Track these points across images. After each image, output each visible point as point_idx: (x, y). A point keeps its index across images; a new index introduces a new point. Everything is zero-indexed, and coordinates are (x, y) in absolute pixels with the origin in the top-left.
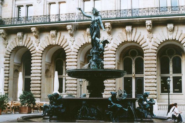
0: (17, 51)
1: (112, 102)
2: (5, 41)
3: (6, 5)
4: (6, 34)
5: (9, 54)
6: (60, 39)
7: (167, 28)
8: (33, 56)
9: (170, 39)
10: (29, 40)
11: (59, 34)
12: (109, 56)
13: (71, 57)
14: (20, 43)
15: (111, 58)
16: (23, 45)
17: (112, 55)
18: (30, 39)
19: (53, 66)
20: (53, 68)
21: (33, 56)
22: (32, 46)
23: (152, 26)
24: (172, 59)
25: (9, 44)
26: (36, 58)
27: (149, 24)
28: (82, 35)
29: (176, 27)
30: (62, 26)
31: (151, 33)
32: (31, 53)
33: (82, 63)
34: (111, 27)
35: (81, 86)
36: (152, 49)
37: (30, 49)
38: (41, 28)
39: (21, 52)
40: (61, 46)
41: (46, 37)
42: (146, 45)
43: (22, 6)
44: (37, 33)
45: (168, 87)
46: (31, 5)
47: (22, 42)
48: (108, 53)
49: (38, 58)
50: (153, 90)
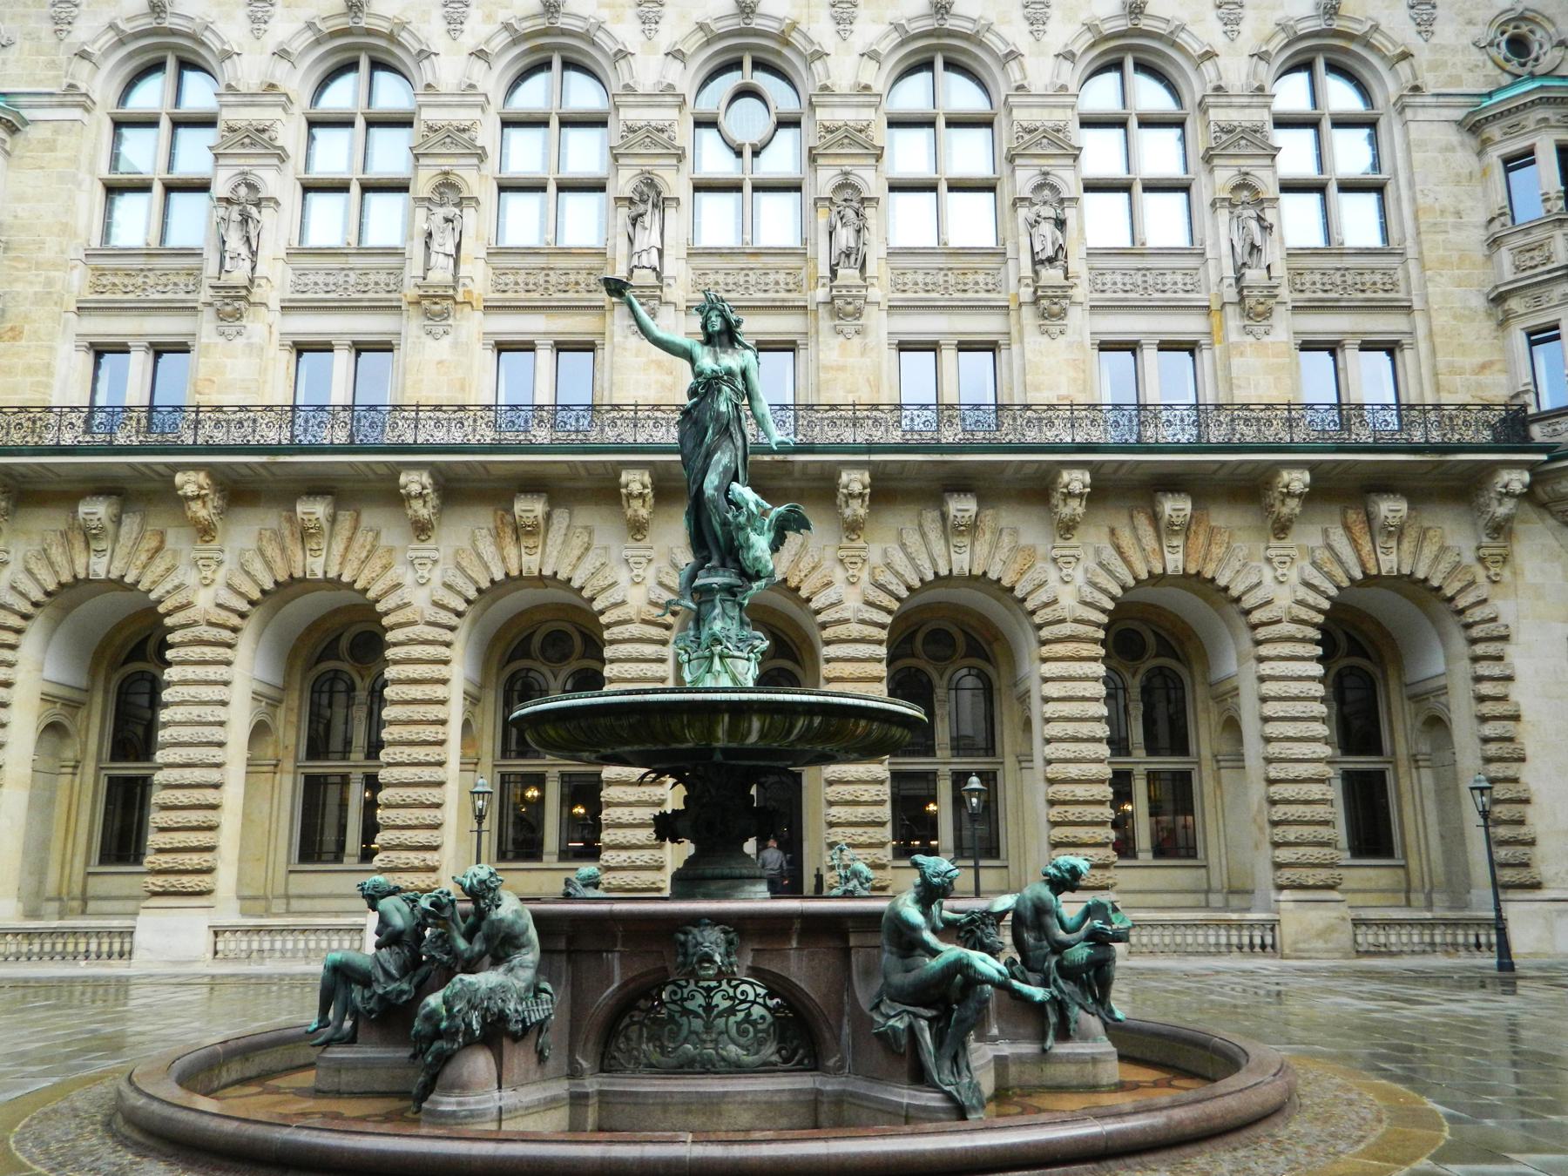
0: (66, 610)
1: (928, 936)
3: (12, 329)
6: (356, 546)
7: (944, 517)
8: (182, 644)
9: (955, 572)
10: (158, 550)
11: (345, 518)
12: (635, 655)
13: (417, 651)
14: (93, 559)
15: (643, 666)
16: (114, 575)
17: (649, 650)
18: (162, 542)
19: (295, 704)
20: (294, 719)
21: (182, 644)
22: (176, 582)
23: (867, 498)
24: (945, 682)
26: (195, 652)
27: (856, 488)
28: (485, 532)
29: (988, 514)
30: (372, 476)
31: (862, 539)
32: (168, 621)
33: (471, 689)
34: (651, 495)
35: (480, 824)
36: (863, 622)
37: (159, 601)
38: (235, 482)
39: (99, 612)
40: (358, 586)
41: (268, 533)
42: (834, 598)
43: (123, 349)
44: (210, 505)
45: (930, 826)
46: (183, 348)
47: (105, 560)
48: (627, 635)
49: (209, 652)
50: (870, 846)
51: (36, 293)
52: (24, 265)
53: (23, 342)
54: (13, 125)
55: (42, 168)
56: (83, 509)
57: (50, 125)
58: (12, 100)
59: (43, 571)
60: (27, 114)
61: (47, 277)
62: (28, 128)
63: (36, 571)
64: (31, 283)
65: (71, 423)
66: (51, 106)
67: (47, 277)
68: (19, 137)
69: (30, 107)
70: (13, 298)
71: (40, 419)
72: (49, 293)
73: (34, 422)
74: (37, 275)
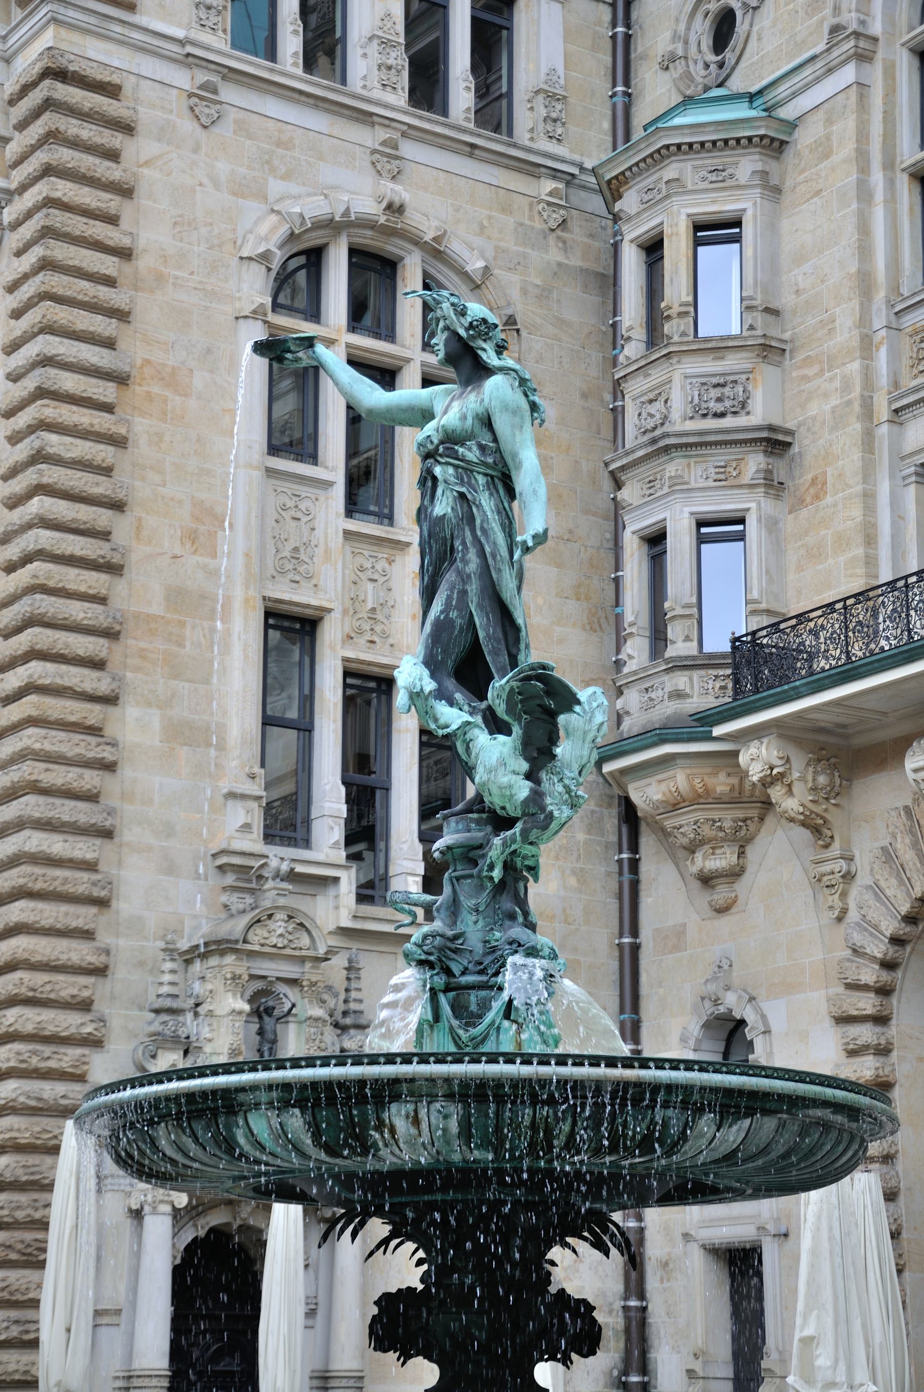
2: (829, 854)
3: (814, 482)
4: (822, 780)
5: (865, 988)
25: (863, 878)
51: (833, 410)
52: (816, 368)
53: (829, 499)
54: (773, 140)
55: (818, 193)
56: (911, 763)
57: (820, 115)
58: (769, 96)
59: (894, 881)
60: (786, 112)
61: (844, 377)
62: (797, 133)
63: (882, 884)
64: (826, 395)
65: (860, 623)
66: (818, 80)
67: (844, 377)
68: (789, 154)
69: (795, 95)
70: (809, 430)
71: (823, 627)
72: (849, 403)
73: (817, 637)
74: (831, 379)
